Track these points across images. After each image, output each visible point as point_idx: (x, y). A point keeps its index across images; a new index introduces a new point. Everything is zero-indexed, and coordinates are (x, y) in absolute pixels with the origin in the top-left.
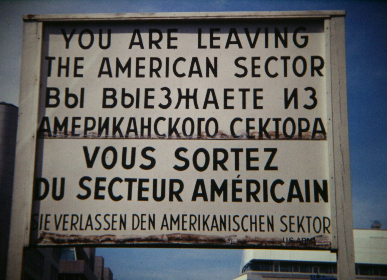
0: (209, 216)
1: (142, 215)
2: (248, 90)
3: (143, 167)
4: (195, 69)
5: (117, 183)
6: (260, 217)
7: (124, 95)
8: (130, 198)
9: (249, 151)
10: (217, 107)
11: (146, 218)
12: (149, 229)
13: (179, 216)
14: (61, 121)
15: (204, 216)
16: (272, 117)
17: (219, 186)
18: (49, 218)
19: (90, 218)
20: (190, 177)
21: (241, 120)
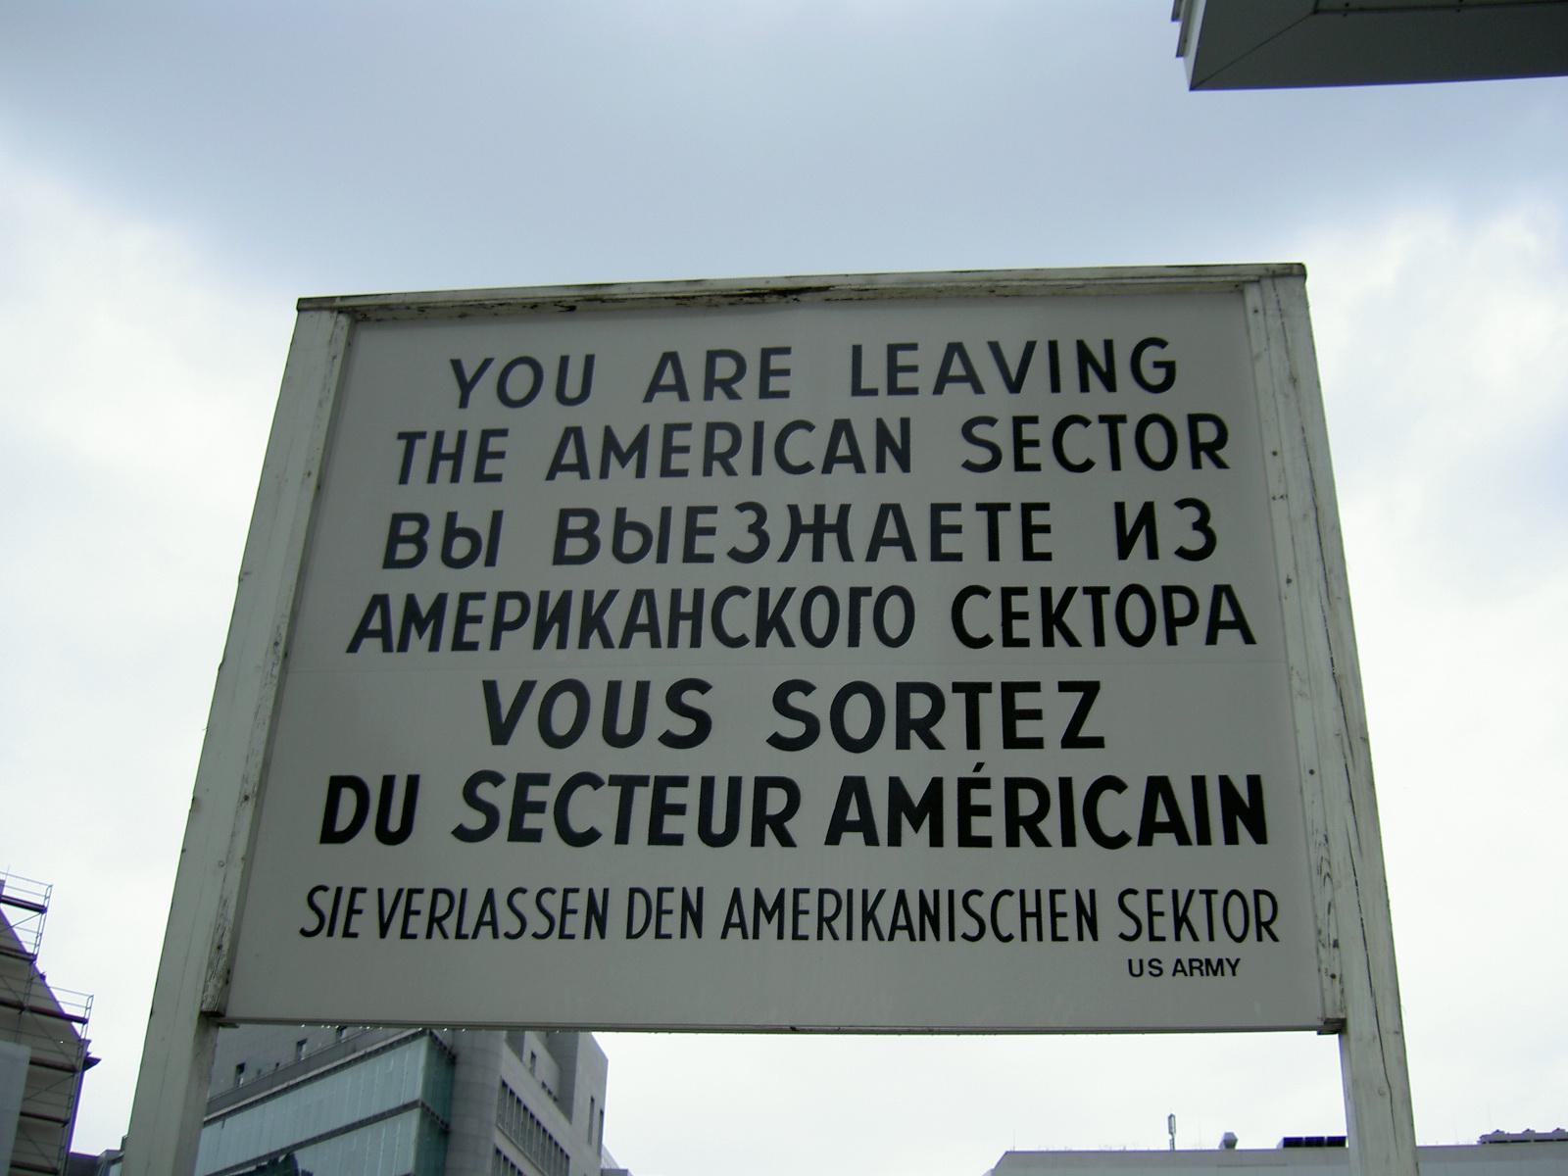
0: (882, 893)
1: (661, 891)
2: (1006, 507)
3: (670, 740)
4: (843, 449)
5: (583, 792)
6: (1053, 893)
7: (622, 524)
8: (622, 837)
9: (1009, 690)
10: (910, 556)
11: (673, 902)
12: (683, 935)
13: (782, 892)
14: (424, 608)
15: (865, 893)
16: (1080, 585)
17: (916, 794)
18: (361, 901)
19: (490, 896)
20: (820, 771)
21: (985, 593)
